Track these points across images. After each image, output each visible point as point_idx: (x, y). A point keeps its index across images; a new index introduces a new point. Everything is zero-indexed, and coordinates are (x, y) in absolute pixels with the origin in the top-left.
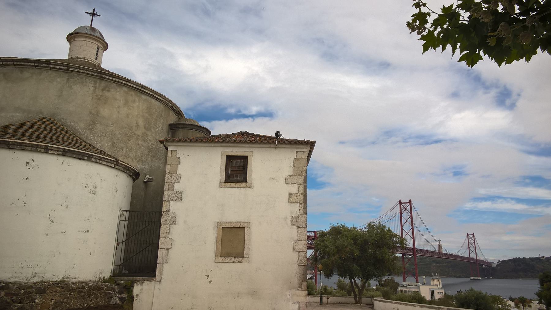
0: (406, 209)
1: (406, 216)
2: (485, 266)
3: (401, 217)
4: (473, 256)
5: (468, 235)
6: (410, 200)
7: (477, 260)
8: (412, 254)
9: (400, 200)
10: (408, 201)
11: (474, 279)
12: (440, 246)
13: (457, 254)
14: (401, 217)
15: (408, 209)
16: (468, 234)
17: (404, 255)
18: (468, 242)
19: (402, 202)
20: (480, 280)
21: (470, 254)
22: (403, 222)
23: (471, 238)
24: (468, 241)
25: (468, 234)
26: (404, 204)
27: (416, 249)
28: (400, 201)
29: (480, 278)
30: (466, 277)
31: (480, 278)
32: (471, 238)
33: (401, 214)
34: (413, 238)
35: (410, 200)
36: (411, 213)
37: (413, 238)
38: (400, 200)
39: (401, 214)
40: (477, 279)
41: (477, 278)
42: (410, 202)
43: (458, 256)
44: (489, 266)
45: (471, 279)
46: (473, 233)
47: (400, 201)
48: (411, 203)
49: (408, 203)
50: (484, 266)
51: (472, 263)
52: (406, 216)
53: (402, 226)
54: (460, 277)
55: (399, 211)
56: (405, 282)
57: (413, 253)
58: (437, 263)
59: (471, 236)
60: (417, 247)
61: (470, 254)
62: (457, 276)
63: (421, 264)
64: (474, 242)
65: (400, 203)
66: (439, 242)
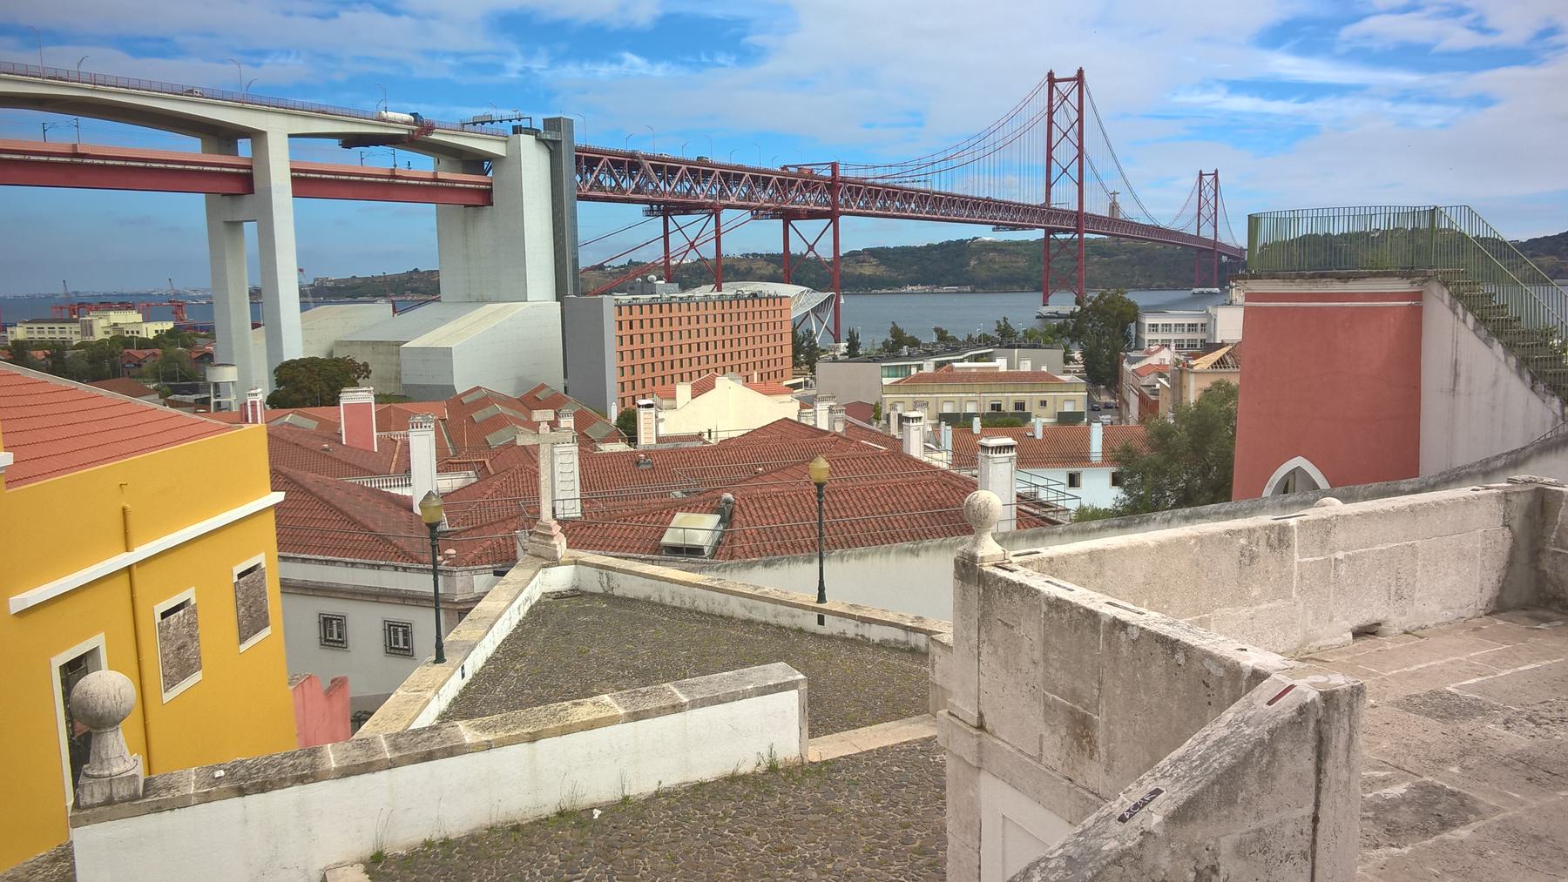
0: (1066, 98)
1: (1064, 118)
2: (1229, 257)
3: (1050, 122)
4: (1207, 232)
5: (1201, 174)
6: (1080, 72)
7: (1215, 243)
9: (1051, 71)
10: (1073, 74)
11: (1202, 293)
12: (1114, 207)
13: (1172, 227)
14: (1050, 122)
15: (1074, 98)
16: (1201, 172)
17: (1049, 231)
18: (1200, 195)
19: (1056, 77)
20: (1216, 293)
21: (1199, 227)
22: (1056, 135)
23: (1208, 186)
24: (1200, 191)
25: (1201, 172)
26: (1058, 84)
28: (1050, 75)
29: (1217, 290)
30: (1175, 288)
31: (1217, 289)
32: (1208, 186)
33: (1050, 113)
34: (1080, 184)
35: (1080, 72)
36: (1080, 111)
37: (1080, 184)
38: (1051, 71)
39: (1050, 113)
40: (1210, 293)
41: (1207, 289)
42: (1080, 78)
43: (1177, 234)
44: (1239, 259)
45: (1194, 293)
46: (1216, 171)
47: (1050, 75)
48: (1082, 81)
49: (1074, 79)
50: (1224, 258)
51: (1201, 250)
52: (1064, 118)
53: (1050, 149)
54: (1160, 288)
55: (1046, 104)
56: (1047, 305)
58: (1104, 255)
59: (1207, 179)
60: (1086, 209)
61: (1199, 227)
62: (1154, 285)
63: (1061, 259)
64: (1216, 195)
65: (1051, 80)
66: (1114, 198)
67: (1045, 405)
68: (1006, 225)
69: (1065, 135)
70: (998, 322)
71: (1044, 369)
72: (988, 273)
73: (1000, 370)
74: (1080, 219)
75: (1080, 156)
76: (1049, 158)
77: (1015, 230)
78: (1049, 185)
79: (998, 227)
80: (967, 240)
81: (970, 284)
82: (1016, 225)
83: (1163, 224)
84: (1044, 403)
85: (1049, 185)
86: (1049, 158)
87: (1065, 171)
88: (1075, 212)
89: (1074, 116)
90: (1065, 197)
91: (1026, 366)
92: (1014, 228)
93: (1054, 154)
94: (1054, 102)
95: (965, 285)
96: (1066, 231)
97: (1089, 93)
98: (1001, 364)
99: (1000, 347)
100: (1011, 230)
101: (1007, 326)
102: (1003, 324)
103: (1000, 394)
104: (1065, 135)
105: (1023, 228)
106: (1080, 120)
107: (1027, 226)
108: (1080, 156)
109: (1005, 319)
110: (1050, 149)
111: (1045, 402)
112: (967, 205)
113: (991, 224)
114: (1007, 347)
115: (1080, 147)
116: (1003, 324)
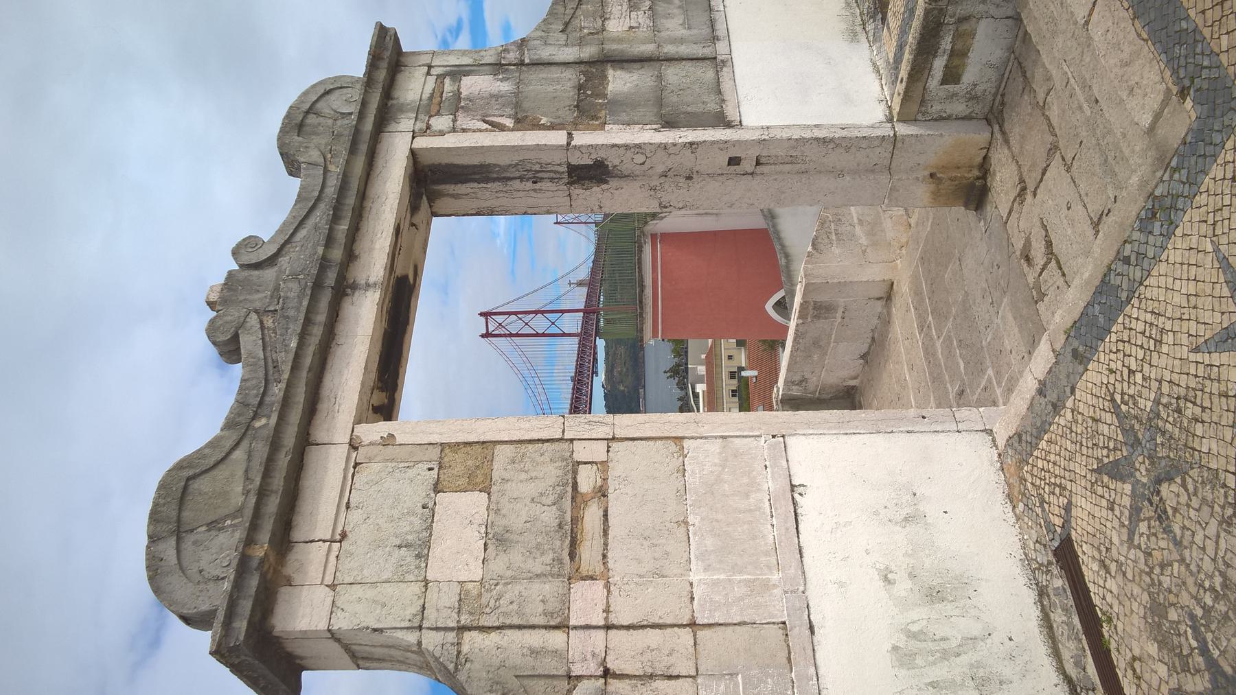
0: (500, 324)
1: (514, 325)
3: (517, 335)
6: (481, 314)
8: (597, 317)
10: (483, 319)
12: (580, 284)
14: (517, 335)
15: (500, 319)
16: (555, 223)
18: (572, 223)
22: (527, 330)
24: (569, 223)
25: (555, 223)
26: (490, 330)
27: (585, 307)
28: (483, 336)
33: (511, 335)
34: (563, 312)
35: (481, 314)
36: (509, 313)
37: (563, 312)
39: (511, 335)
42: (485, 315)
47: (483, 336)
49: (487, 319)
52: (514, 325)
53: (537, 335)
57: (594, 313)
65: (487, 335)
66: (573, 284)
67: (732, 356)
68: (593, 367)
69: (527, 324)
70: (668, 378)
71: (703, 356)
72: (630, 377)
73: (705, 389)
74: (589, 311)
75: (543, 312)
76: (544, 335)
77: (597, 360)
78: (564, 335)
79: (595, 373)
80: (605, 393)
81: (638, 391)
82: (594, 359)
83: (592, 249)
84: (730, 357)
85: (564, 335)
86: (544, 335)
87: (553, 323)
88: (584, 315)
89: (513, 317)
90: (572, 323)
91: (702, 370)
92: (595, 360)
93: (540, 332)
94: (502, 333)
95: (639, 393)
96: (598, 321)
97: (497, 307)
98: (701, 388)
99: (687, 379)
100: (597, 363)
101: (671, 370)
102: (669, 374)
103: (724, 390)
104: (527, 324)
105: (595, 353)
106: (516, 313)
107: (594, 351)
108: (543, 312)
109: (665, 372)
110: (537, 335)
111: (729, 356)
112: (579, 388)
113: (592, 378)
114: (687, 373)
115: (536, 312)
116: (669, 374)
